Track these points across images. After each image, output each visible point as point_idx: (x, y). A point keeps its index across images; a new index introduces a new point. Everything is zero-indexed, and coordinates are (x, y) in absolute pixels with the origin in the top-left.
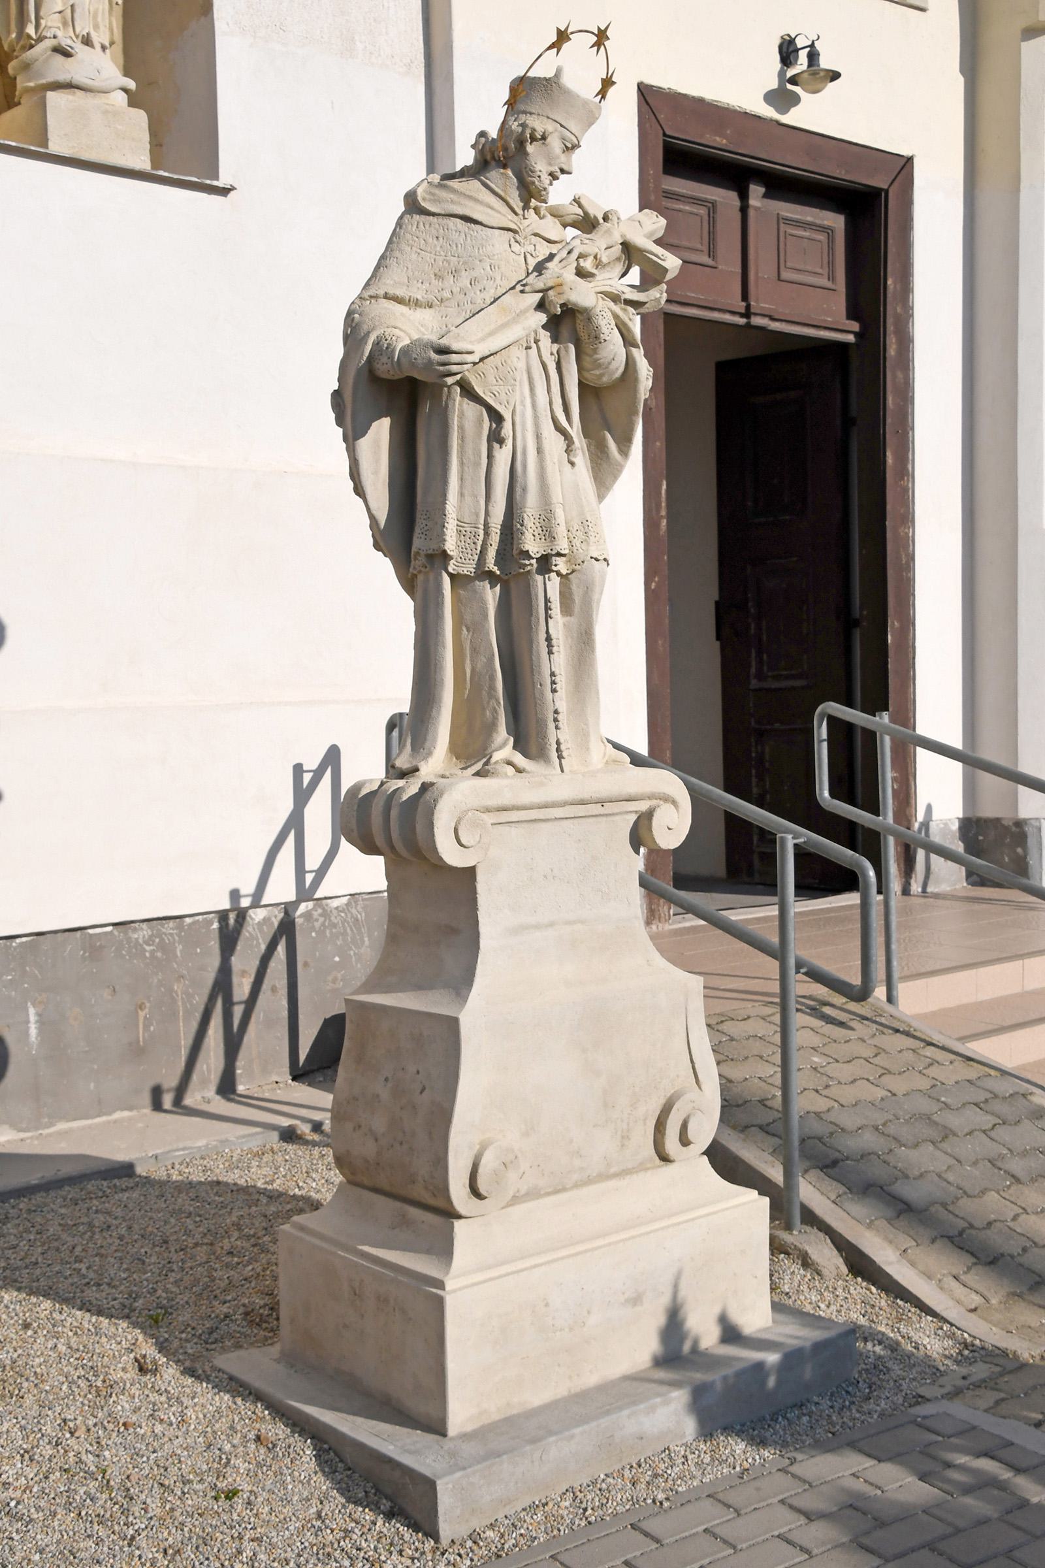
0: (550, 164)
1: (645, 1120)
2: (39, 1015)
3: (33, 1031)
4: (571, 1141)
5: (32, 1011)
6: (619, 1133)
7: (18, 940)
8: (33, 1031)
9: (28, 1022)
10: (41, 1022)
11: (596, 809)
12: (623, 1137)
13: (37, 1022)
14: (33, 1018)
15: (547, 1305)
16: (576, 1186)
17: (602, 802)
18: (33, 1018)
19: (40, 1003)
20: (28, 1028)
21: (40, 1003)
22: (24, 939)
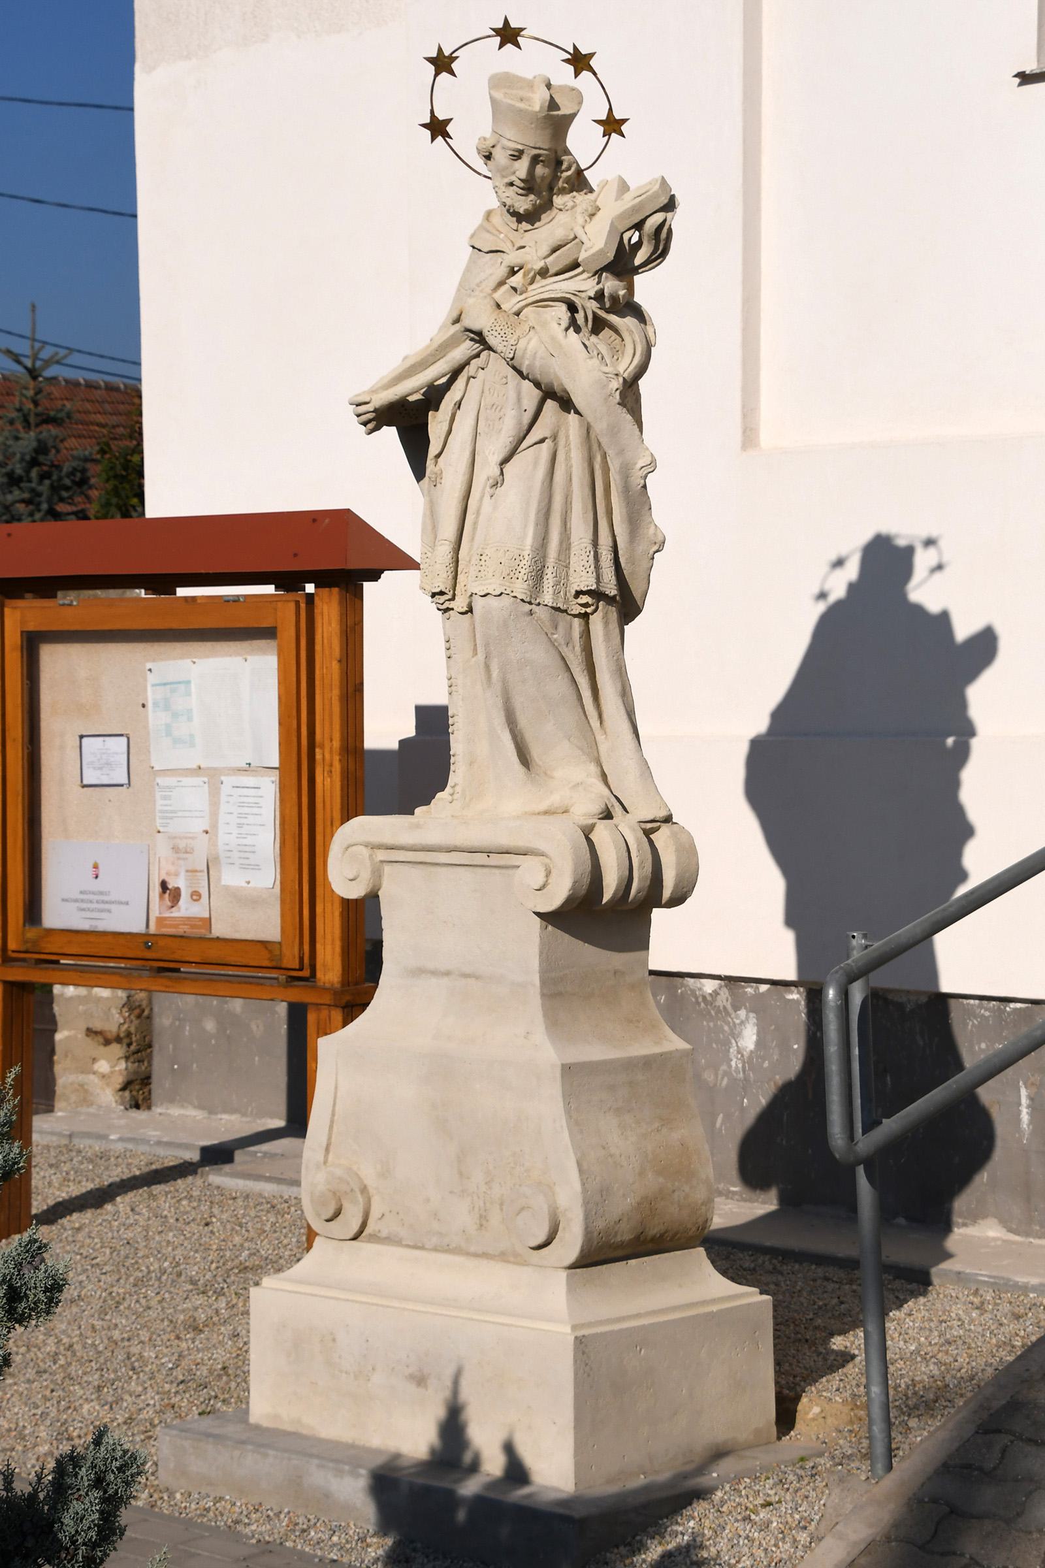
0: (503, 177)
1: (501, 1204)
2: (1031, 1098)
3: (1025, 1116)
4: (428, 1200)
5: (1024, 1092)
6: (476, 1210)
7: (1012, 1005)
8: (1025, 1116)
9: (1020, 1104)
10: (1033, 1107)
11: (480, 858)
12: (481, 1216)
13: (1028, 1107)
14: (1024, 1101)
15: (334, 1340)
16: (435, 1249)
17: (489, 852)
18: (1024, 1101)
19: (1033, 1084)
20: (1019, 1112)
21: (1033, 1084)
22: (1019, 1005)
